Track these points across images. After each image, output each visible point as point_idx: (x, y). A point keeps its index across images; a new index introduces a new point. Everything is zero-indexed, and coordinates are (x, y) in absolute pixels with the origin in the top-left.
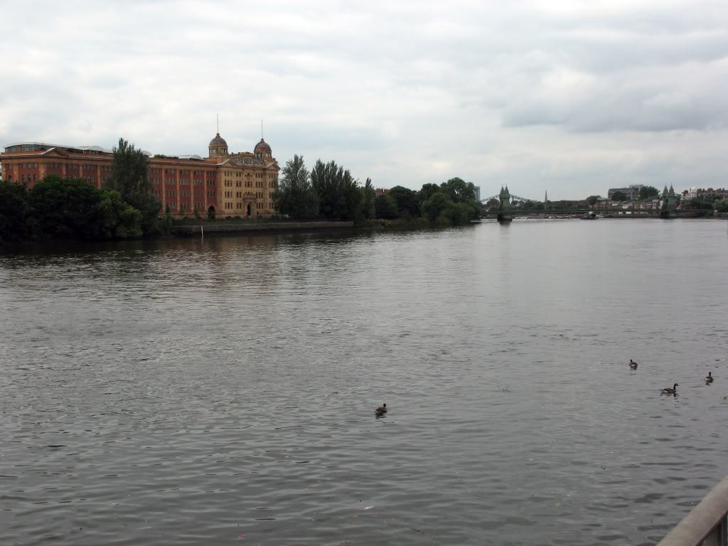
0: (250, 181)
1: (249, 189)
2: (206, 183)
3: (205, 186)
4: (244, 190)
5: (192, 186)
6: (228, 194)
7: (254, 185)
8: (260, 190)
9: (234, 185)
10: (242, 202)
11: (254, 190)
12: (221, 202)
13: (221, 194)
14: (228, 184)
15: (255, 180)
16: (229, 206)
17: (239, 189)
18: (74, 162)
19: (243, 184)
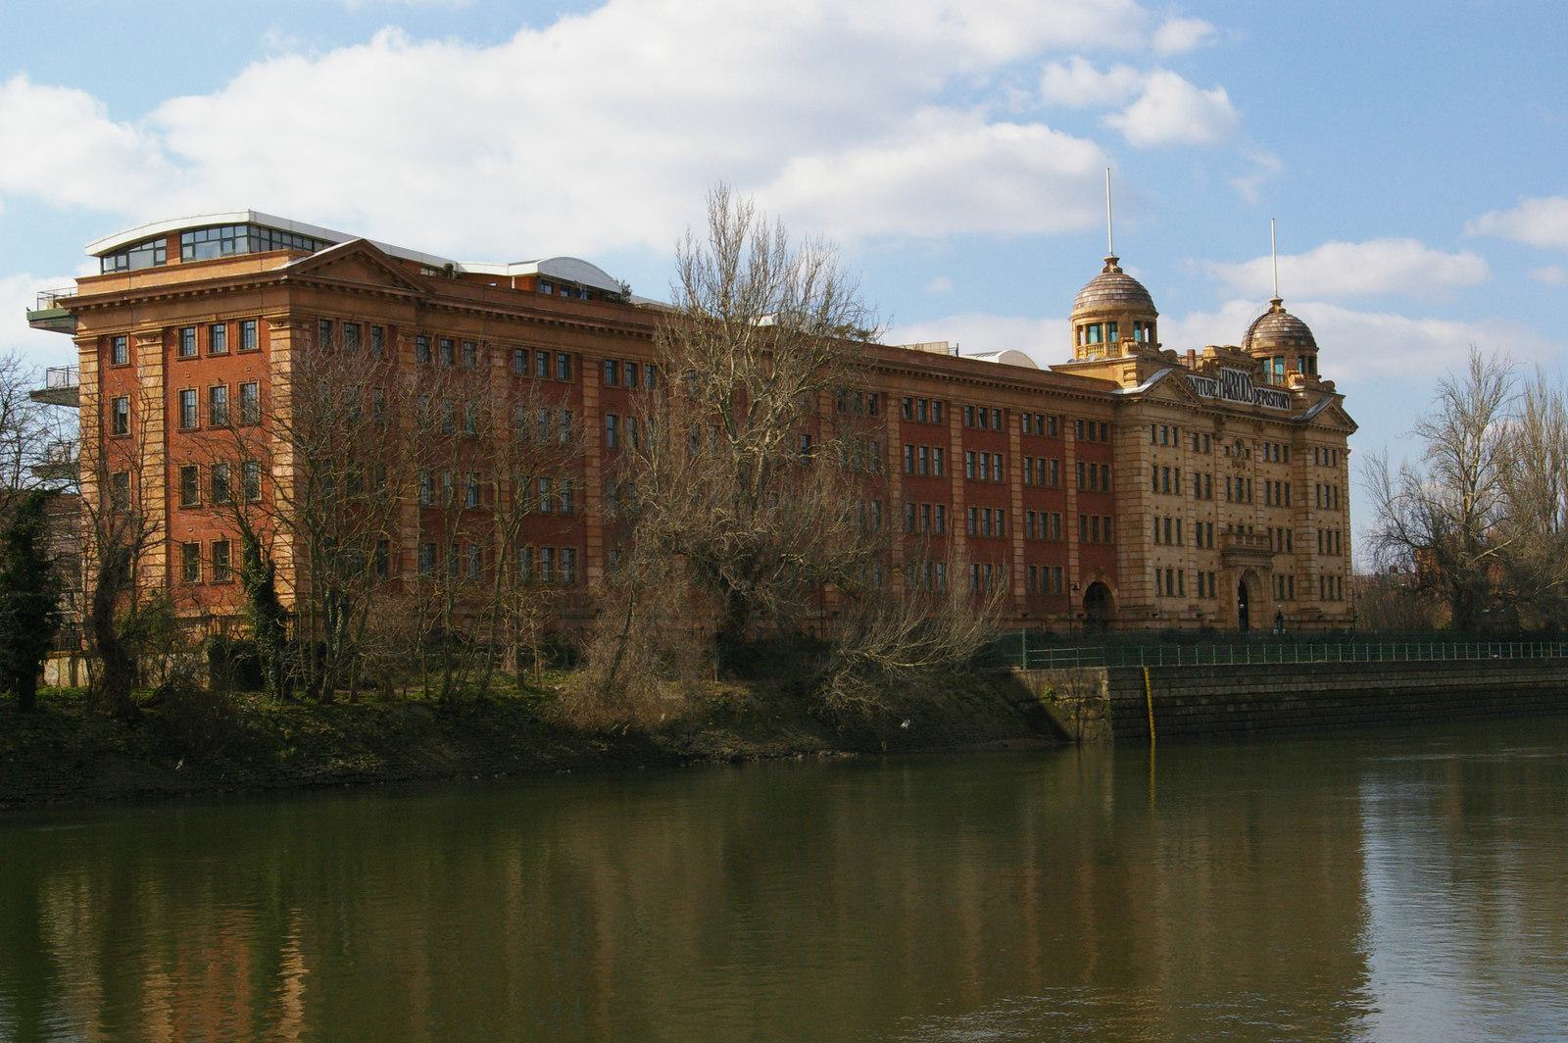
0: (1246, 474)
1: (1240, 513)
3: (1072, 492)
4: (1224, 513)
8: (1280, 518)
10: (1215, 567)
11: (1261, 517)
12: (1140, 565)
13: (1138, 526)
14: (1166, 481)
15: (1266, 470)
16: (1170, 579)
19: (1220, 490)
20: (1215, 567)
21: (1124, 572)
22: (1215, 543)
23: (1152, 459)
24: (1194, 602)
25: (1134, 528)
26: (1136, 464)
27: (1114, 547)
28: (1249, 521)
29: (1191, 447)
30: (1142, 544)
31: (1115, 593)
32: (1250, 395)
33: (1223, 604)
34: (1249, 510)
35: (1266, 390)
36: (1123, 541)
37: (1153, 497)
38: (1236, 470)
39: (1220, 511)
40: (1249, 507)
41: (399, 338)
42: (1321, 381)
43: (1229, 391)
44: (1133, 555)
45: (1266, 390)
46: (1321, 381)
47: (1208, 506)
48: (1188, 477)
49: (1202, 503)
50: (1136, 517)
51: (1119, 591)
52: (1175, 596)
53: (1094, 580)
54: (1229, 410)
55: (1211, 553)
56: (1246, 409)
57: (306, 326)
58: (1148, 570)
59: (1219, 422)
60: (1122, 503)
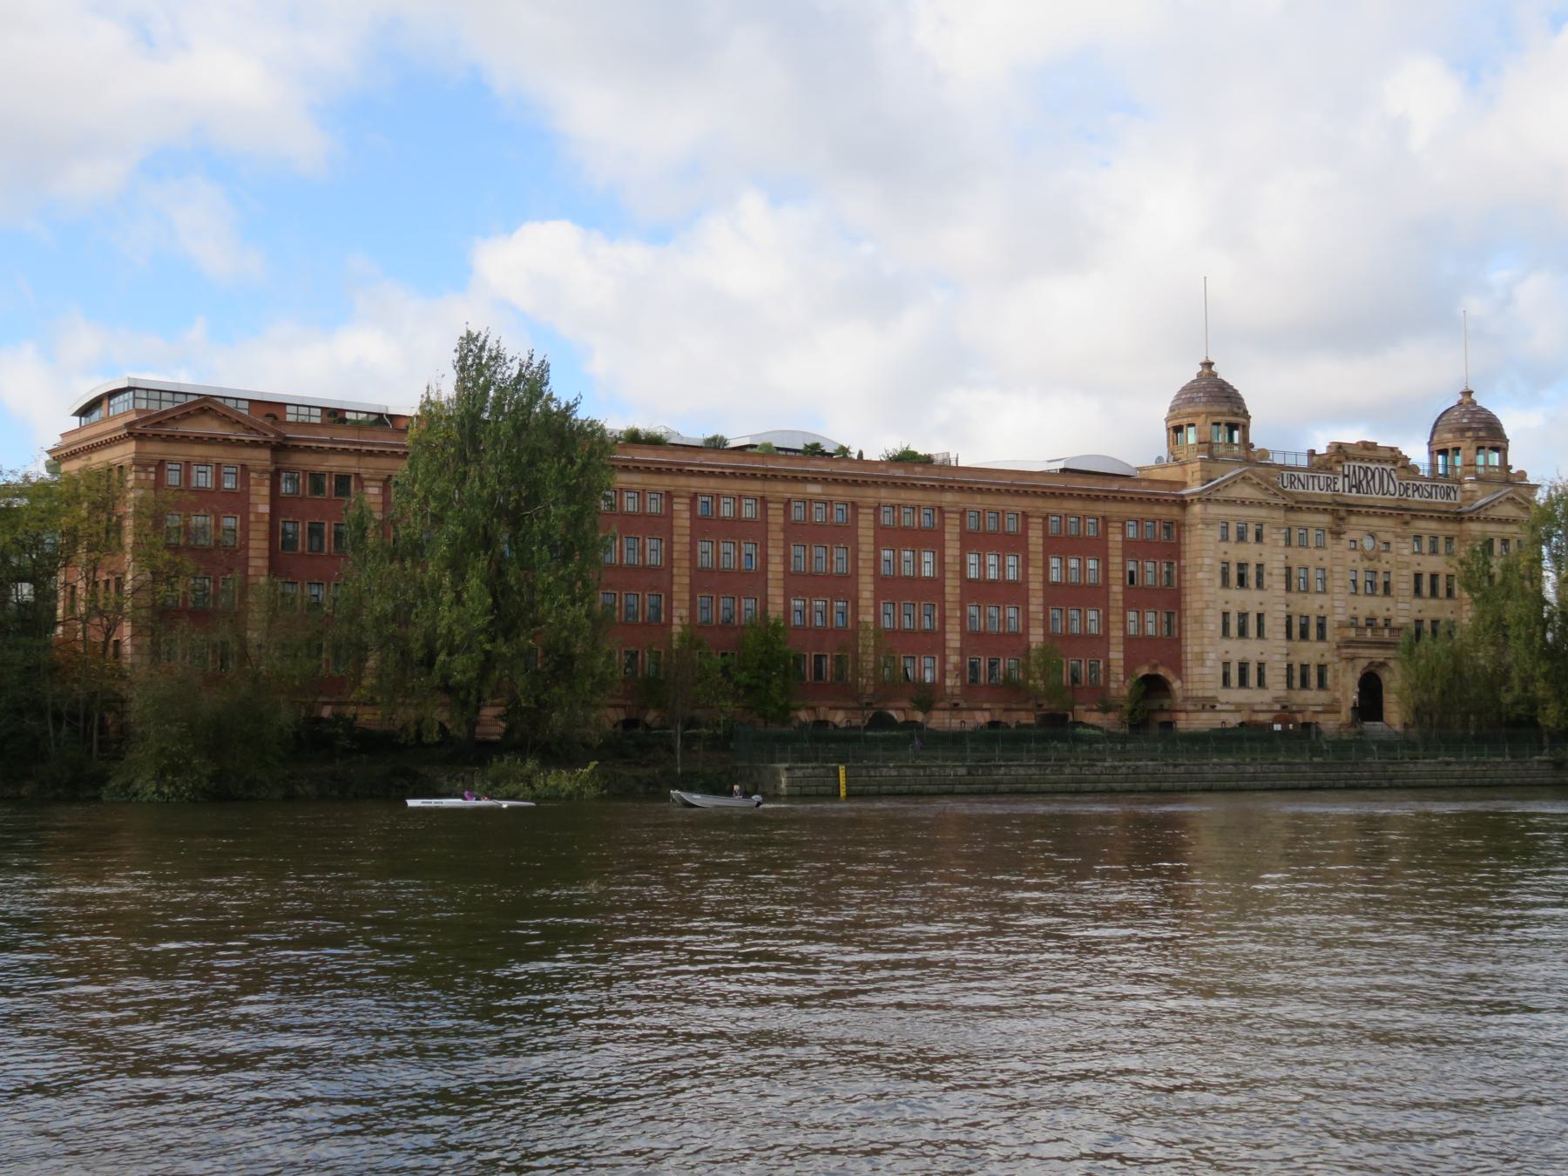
0: (1382, 567)
2: (1116, 574)
4: (1339, 606)
5: (1035, 584)
6: (1242, 626)
7: (1403, 584)
9: (1275, 582)
12: (1201, 658)
13: (1199, 620)
17: (1311, 605)
18: (335, 464)
19: (1339, 584)
20: (1328, 658)
21: (1189, 664)
22: (1329, 634)
23: (1223, 556)
25: (1196, 622)
26: (1199, 561)
27: (1179, 640)
28: (1386, 614)
29: (1282, 543)
30: (1202, 637)
31: (1176, 685)
32: (1392, 489)
33: (1338, 695)
34: (1388, 602)
35: (1418, 483)
36: (1189, 634)
37: (1222, 592)
38: (1366, 564)
39: (1336, 603)
40: (1387, 599)
41: (253, 475)
42: (1513, 471)
43: (1358, 487)
44: (1196, 649)
45: (1418, 483)
46: (1513, 471)
47: (1320, 600)
48: (1276, 572)
50: (1197, 613)
54: (1348, 505)
55: (1321, 646)
57: (153, 469)
58: (1209, 663)
60: (1188, 599)
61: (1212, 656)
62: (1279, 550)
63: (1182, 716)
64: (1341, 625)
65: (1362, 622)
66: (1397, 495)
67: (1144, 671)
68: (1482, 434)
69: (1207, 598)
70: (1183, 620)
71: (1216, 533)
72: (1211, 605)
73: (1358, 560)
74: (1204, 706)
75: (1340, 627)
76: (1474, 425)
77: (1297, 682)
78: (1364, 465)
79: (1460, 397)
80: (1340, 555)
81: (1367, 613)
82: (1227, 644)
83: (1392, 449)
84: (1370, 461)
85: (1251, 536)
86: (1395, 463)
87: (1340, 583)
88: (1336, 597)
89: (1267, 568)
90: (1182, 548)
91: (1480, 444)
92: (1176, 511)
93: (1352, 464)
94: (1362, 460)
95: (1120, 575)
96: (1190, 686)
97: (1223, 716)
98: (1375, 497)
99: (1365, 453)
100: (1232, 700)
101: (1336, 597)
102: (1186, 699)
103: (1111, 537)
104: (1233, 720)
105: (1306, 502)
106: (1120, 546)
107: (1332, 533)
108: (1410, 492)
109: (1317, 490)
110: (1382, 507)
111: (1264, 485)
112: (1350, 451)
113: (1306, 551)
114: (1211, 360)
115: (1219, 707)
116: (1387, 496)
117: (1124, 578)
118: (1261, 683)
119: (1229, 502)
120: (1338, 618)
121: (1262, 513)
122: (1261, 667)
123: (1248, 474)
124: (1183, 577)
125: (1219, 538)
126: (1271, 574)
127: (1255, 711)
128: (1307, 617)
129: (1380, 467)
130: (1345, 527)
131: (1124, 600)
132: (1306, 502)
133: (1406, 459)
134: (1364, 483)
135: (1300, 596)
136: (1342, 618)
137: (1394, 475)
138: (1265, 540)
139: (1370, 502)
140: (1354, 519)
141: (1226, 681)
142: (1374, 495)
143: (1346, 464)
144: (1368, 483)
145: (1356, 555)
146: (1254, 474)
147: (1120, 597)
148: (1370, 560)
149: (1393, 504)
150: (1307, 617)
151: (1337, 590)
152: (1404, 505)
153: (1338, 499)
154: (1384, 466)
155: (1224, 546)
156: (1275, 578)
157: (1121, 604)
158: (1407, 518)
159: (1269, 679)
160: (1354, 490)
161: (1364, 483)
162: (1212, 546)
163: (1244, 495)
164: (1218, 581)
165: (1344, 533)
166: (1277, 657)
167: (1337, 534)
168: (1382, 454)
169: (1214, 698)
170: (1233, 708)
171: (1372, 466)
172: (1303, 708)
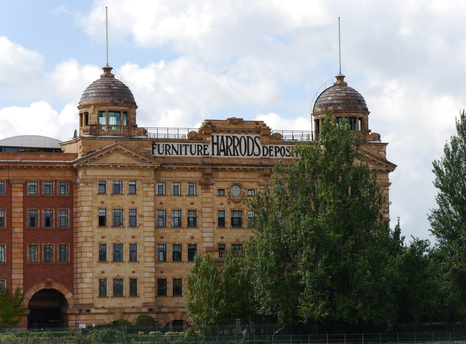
3: (18, 230)
23: (100, 205)
24: (150, 300)
31: (68, 296)
38: (233, 206)
39: (204, 235)
45: (280, 146)
47: (191, 232)
48: (146, 214)
49: (181, 231)
51: (73, 294)
52: (125, 297)
53: (44, 288)
54: (212, 165)
56: (251, 162)
58: (86, 280)
59: (205, 175)
61: (90, 275)
62: (149, 199)
63: (73, 317)
64: (209, 250)
65: (228, 247)
66: (261, 155)
67: (42, 286)
68: (339, 108)
69: (84, 234)
70: (75, 250)
71: (96, 189)
72: (89, 239)
73: (225, 203)
74: (81, 310)
75: (207, 252)
76: (335, 102)
77: (170, 291)
78: (231, 135)
79: (335, 80)
80: (209, 200)
81: (234, 241)
82: (103, 266)
83: (257, 123)
84: (236, 132)
85: (125, 189)
86: (258, 132)
87: (209, 220)
88: (204, 230)
89: (140, 211)
90: (75, 200)
91: (338, 115)
92: (68, 174)
93: (220, 135)
94: (229, 131)
95: (22, 220)
96: (80, 296)
97: (98, 317)
98: (242, 157)
99: (233, 126)
100: (107, 305)
101: (204, 230)
102: (76, 305)
103: (14, 194)
104: (108, 320)
105: (175, 164)
106: (22, 200)
107: (201, 184)
108: (273, 153)
109: (188, 153)
110: (247, 165)
111: (134, 154)
112: (219, 125)
113: (179, 199)
114: (110, 66)
115: (93, 311)
116: (252, 156)
117: (24, 222)
118: (134, 292)
119: (103, 167)
120: (205, 245)
121: (135, 173)
122: (133, 282)
123: (119, 147)
124: (75, 220)
125: (97, 192)
126: (142, 216)
127: (125, 313)
128: (180, 245)
129: (245, 136)
130: (212, 181)
131: (24, 238)
132: (175, 164)
133: (268, 129)
134: (231, 148)
135: (173, 230)
136: (211, 245)
137: (258, 141)
138: (137, 192)
139: (237, 162)
140: (221, 174)
141: (102, 293)
142: (240, 156)
143: (215, 135)
144: (235, 147)
145: (224, 200)
146: (125, 147)
147: (21, 236)
148: (235, 202)
149: (256, 162)
150: (180, 245)
151: (205, 225)
152: (264, 162)
153: (205, 160)
154: (250, 135)
155: (101, 198)
156: (145, 219)
157: (22, 241)
158: (268, 172)
159: (140, 289)
160: (222, 153)
161: (231, 148)
162: (90, 199)
163: (118, 162)
164: (96, 222)
165: (213, 184)
166: (147, 274)
167: (206, 186)
168: (246, 127)
169: (92, 305)
170: (106, 311)
171: (239, 136)
172: (173, 310)
